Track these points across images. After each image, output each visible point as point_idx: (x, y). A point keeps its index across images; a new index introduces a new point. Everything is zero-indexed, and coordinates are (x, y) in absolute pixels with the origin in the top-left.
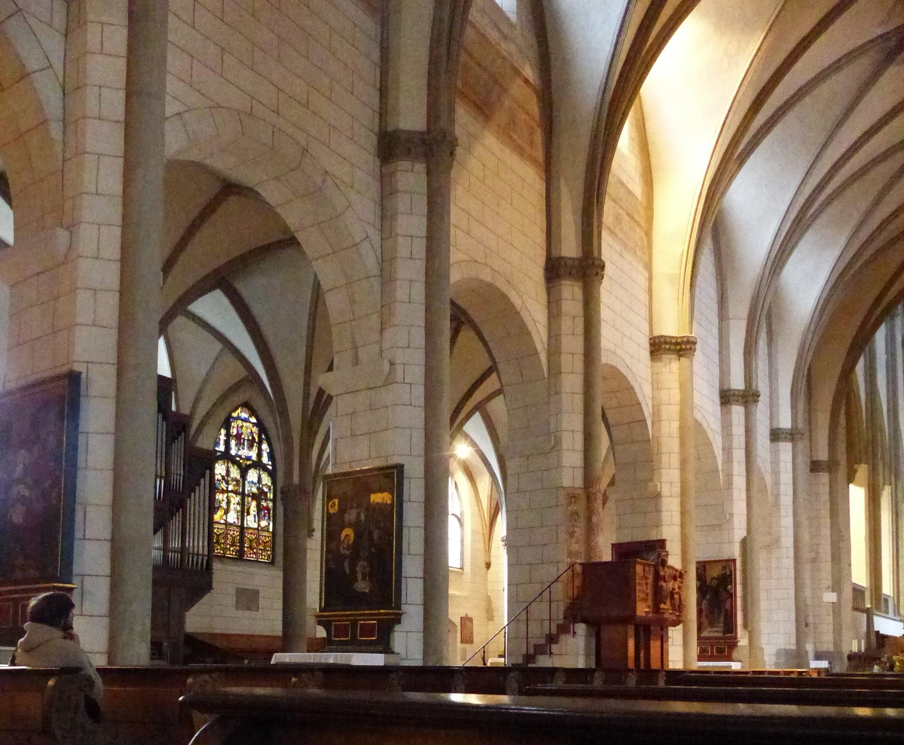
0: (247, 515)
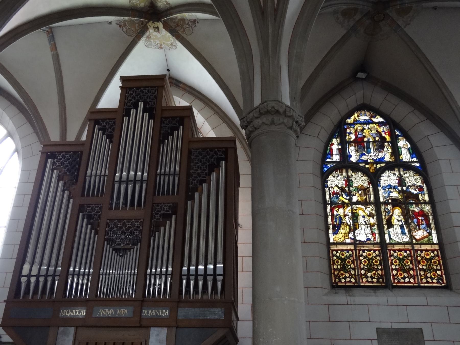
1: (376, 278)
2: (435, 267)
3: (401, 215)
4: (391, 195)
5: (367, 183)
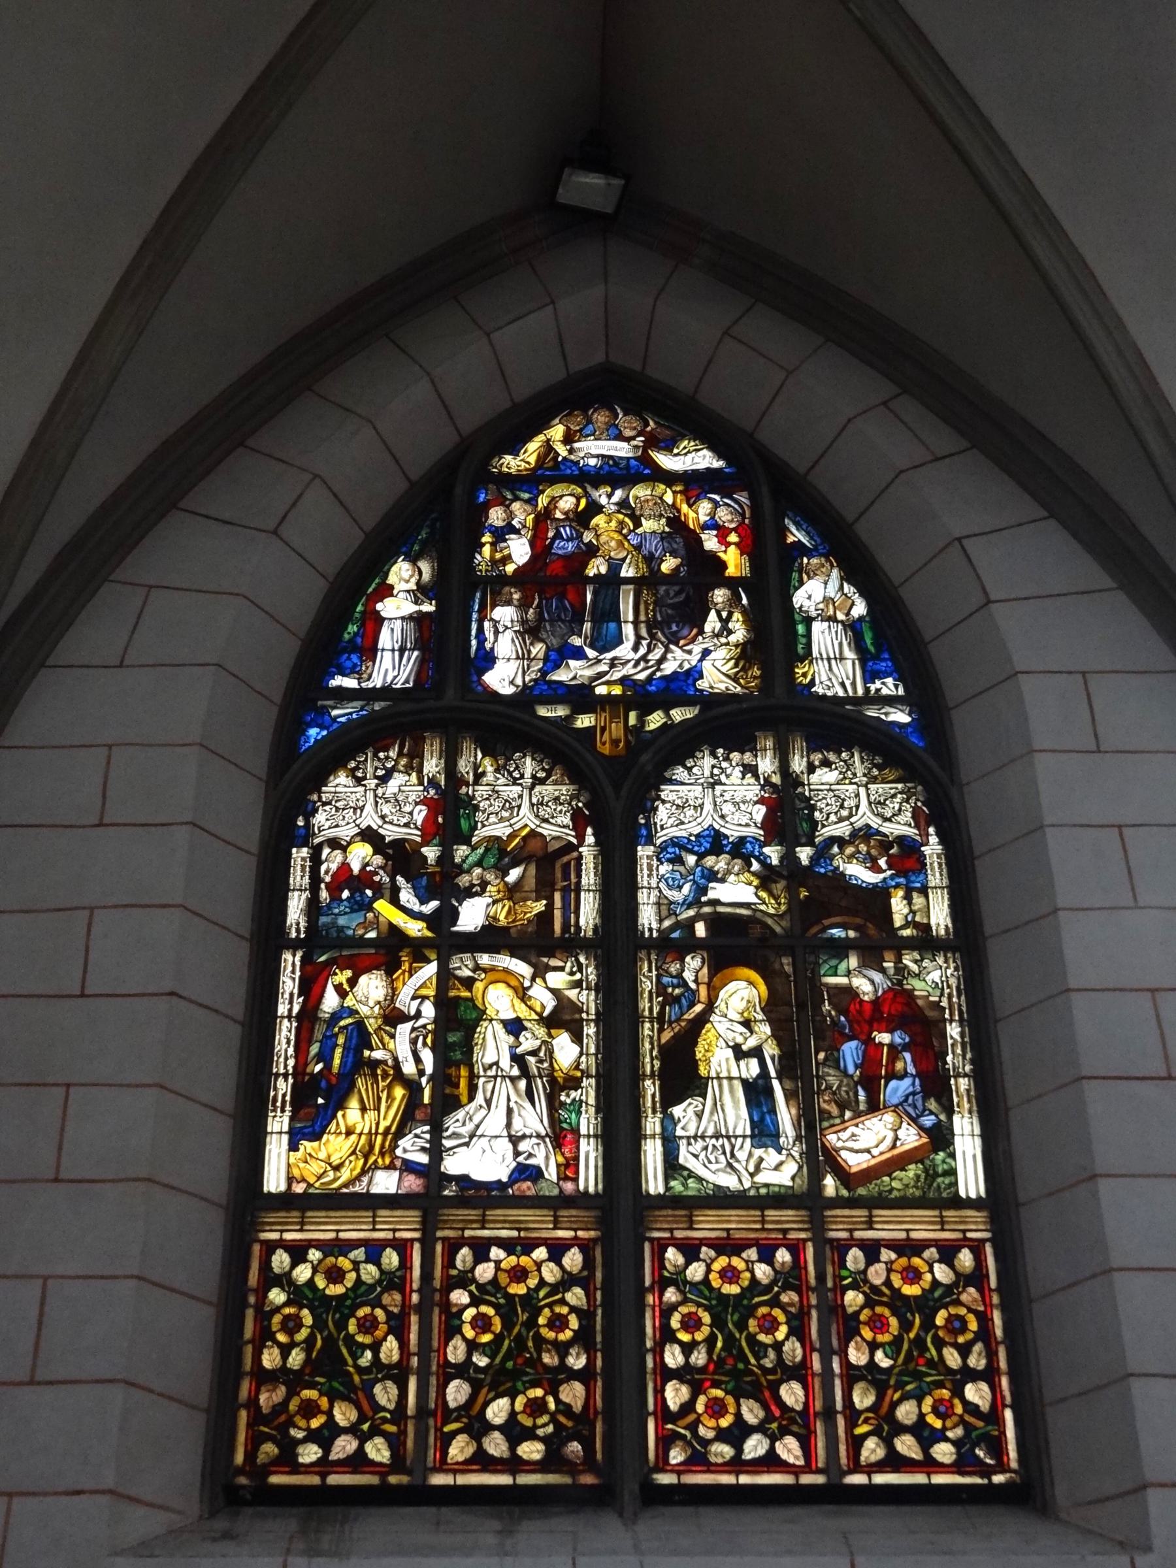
0: (671, 1097)
1: (540, 1432)
2: (952, 1358)
3: (760, 1016)
4: (712, 895)
5: (567, 820)
